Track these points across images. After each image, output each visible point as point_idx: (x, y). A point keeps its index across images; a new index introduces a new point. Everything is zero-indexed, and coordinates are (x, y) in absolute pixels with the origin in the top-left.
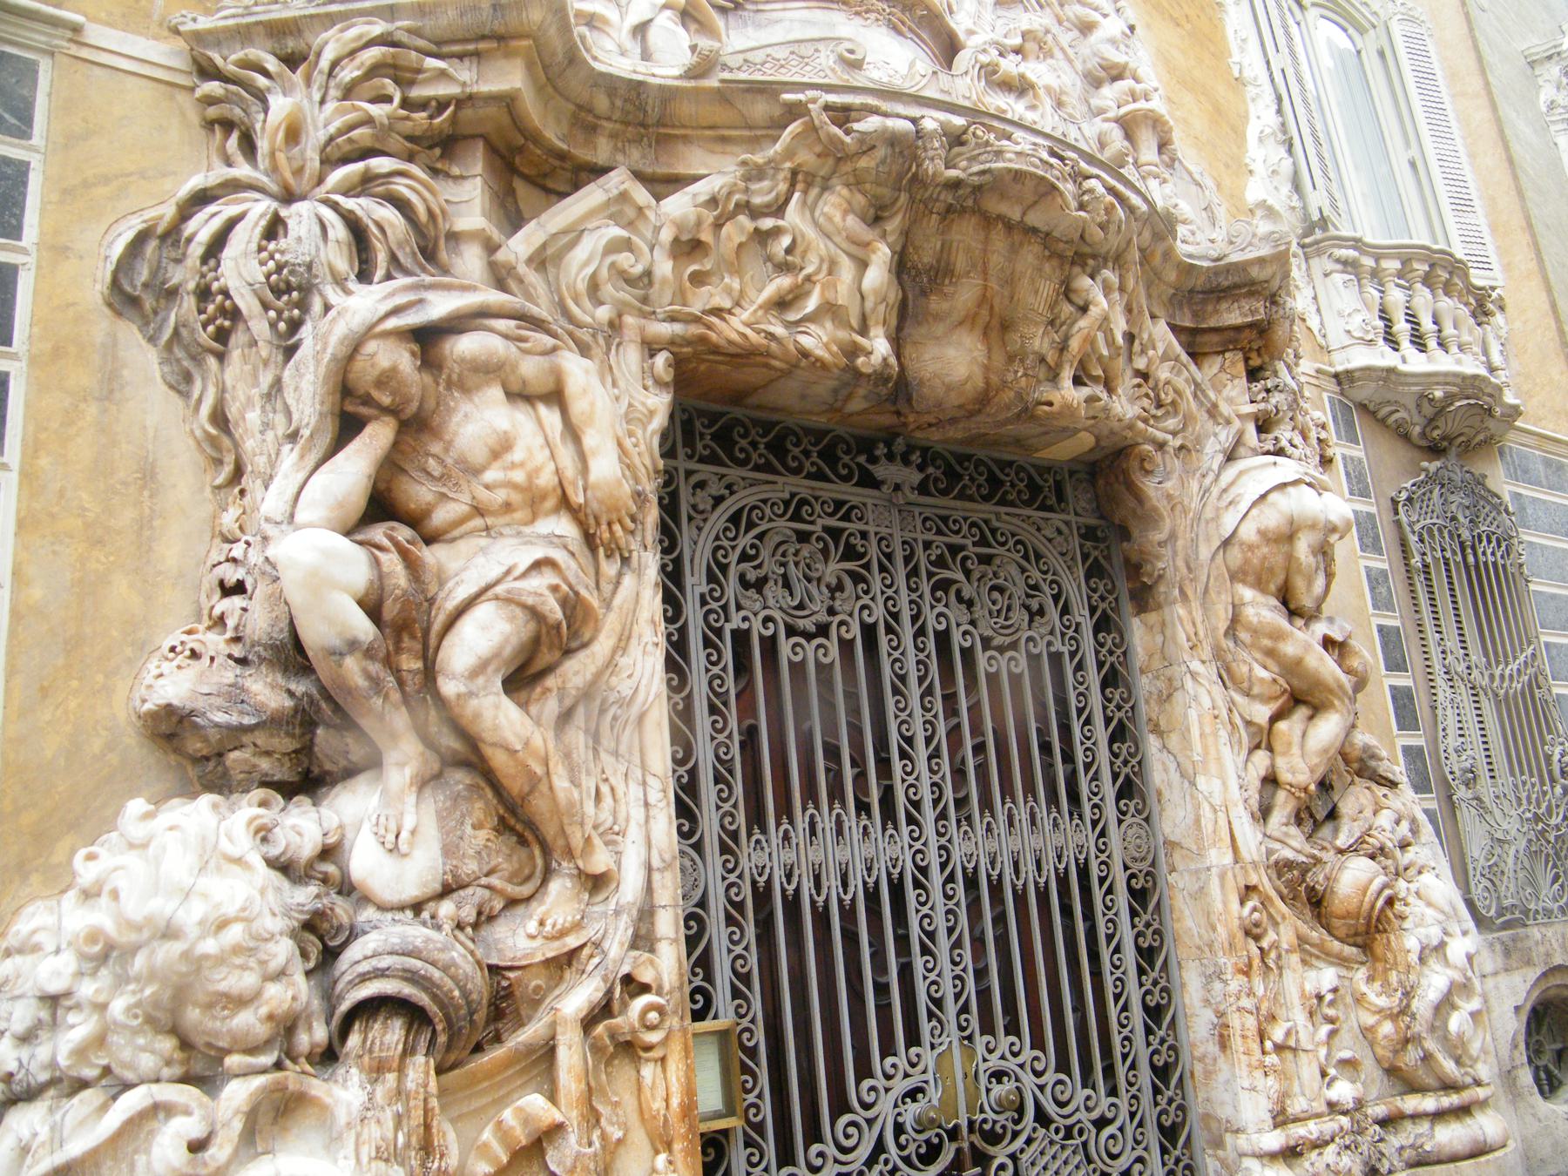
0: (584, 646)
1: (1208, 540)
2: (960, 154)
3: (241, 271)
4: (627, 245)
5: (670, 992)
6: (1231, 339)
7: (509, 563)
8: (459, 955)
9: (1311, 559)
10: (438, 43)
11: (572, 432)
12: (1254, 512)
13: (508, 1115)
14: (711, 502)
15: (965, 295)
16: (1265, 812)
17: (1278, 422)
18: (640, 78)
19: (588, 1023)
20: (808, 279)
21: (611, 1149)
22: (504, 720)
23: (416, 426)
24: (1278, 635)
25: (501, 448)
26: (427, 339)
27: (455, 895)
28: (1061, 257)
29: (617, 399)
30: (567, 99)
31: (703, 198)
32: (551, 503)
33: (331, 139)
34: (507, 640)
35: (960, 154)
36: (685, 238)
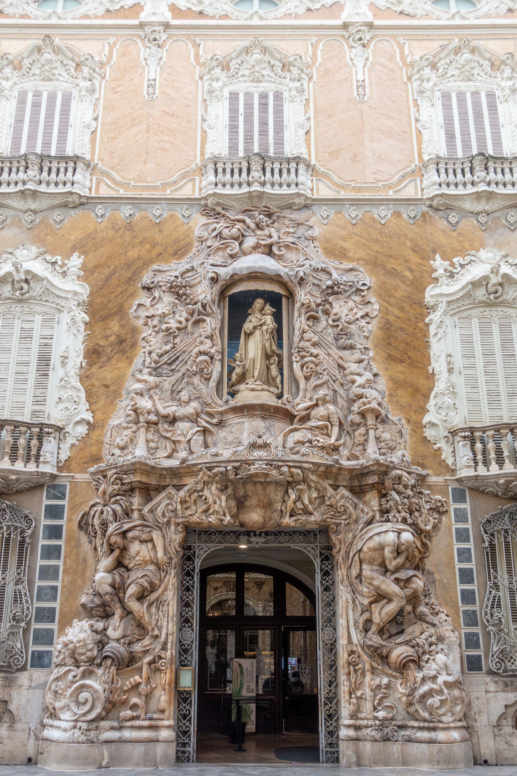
3: (96, 522)
4: (171, 504)
6: (373, 486)
8: (122, 649)
11: (154, 547)
13: (132, 679)
16: (366, 630)
19: (150, 663)
21: (153, 689)
22: (134, 605)
23: (124, 549)
25: (138, 553)
26: (124, 534)
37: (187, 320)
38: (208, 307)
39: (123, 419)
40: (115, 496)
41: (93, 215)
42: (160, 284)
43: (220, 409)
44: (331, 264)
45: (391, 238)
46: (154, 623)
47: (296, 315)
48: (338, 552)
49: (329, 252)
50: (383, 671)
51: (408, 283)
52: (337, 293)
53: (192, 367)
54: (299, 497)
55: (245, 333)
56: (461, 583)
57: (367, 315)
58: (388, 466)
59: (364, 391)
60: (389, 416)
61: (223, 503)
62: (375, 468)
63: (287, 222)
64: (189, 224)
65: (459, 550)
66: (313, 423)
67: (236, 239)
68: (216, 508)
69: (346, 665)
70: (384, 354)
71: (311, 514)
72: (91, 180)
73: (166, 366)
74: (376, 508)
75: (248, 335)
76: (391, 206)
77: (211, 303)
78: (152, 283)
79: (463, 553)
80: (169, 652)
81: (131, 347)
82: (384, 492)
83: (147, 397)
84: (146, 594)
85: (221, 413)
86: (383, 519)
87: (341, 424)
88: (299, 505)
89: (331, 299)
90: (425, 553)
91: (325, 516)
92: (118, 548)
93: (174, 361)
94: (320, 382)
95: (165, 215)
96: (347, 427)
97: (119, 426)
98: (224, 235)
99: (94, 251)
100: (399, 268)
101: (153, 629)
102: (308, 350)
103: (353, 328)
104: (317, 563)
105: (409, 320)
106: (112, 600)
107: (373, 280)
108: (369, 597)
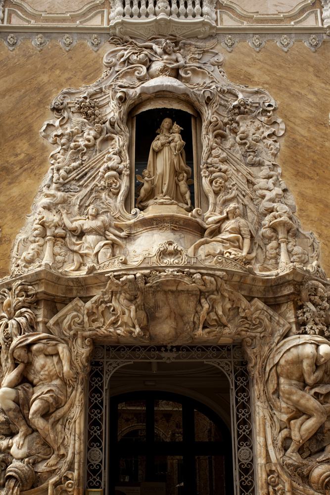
0: (62, 407)
1: (269, 365)
2: (150, 279)
4: (77, 316)
5: (75, 480)
7: (43, 391)
10: (31, 283)
11: (60, 361)
12: (285, 355)
14: (113, 368)
15: (165, 311)
17: (309, 322)
18: (77, 277)
19: (56, 484)
20: (118, 316)
22: (39, 423)
23: (29, 365)
24: (291, 393)
25: (43, 367)
26: (29, 347)
27: (29, 458)
28: (196, 295)
29: (74, 352)
30: (63, 285)
31: (93, 302)
32: (54, 378)
33: (15, 306)
34: (40, 407)
35: (150, 279)
36: (90, 311)
37: (95, 138)
38: (116, 125)
39: (30, 233)
40: (20, 309)
41: (5, 44)
42: (69, 105)
43: (128, 222)
44: (237, 88)
45: (294, 64)
46: (61, 441)
47: (204, 132)
49: (234, 77)
51: (313, 105)
52: (244, 113)
53: (100, 182)
54: (213, 307)
55: (154, 150)
57: (274, 134)
58: (303, 276)
59: (275, 205)
60: (300, 230)
61: (132, 314)
62: (291, 278)
63: (193, 49)
64: (98, 52)
66: (225, 236)
67: (144, 64)
68: (124, 320)
69: (265, 486)
70: (292, 171)
71: (225, 326)
72: (4, 12)
73: (74, 182)
74: (293, 320)
75: (156, 153)
76: (293, 35)
77: (119, 121)
78: (62, 104)
80: (76, 471)
81: (40, 165)
82: (300, 303)
83: (54, 212)
84: (51, 410)
85: (130, 227)
86: (301, 332)
87: (252, 237)
88: (213, 316)
89: (237, 118)
91: (240, 329)
92: (23, 362)
93: (82, 177)
94: (229, 196)
95: (75, 43)
96: (258, 240)
97: (25, 241)
98: (132, 61)
99: (4, 77)
100: (303, 92)
101: (59, 449)
102: (217, 165)
103: (261, 146)
104: (231, 379)
105: (315, 140)
106: (16, 417)
107: (279, 102)
108: (287, 413)
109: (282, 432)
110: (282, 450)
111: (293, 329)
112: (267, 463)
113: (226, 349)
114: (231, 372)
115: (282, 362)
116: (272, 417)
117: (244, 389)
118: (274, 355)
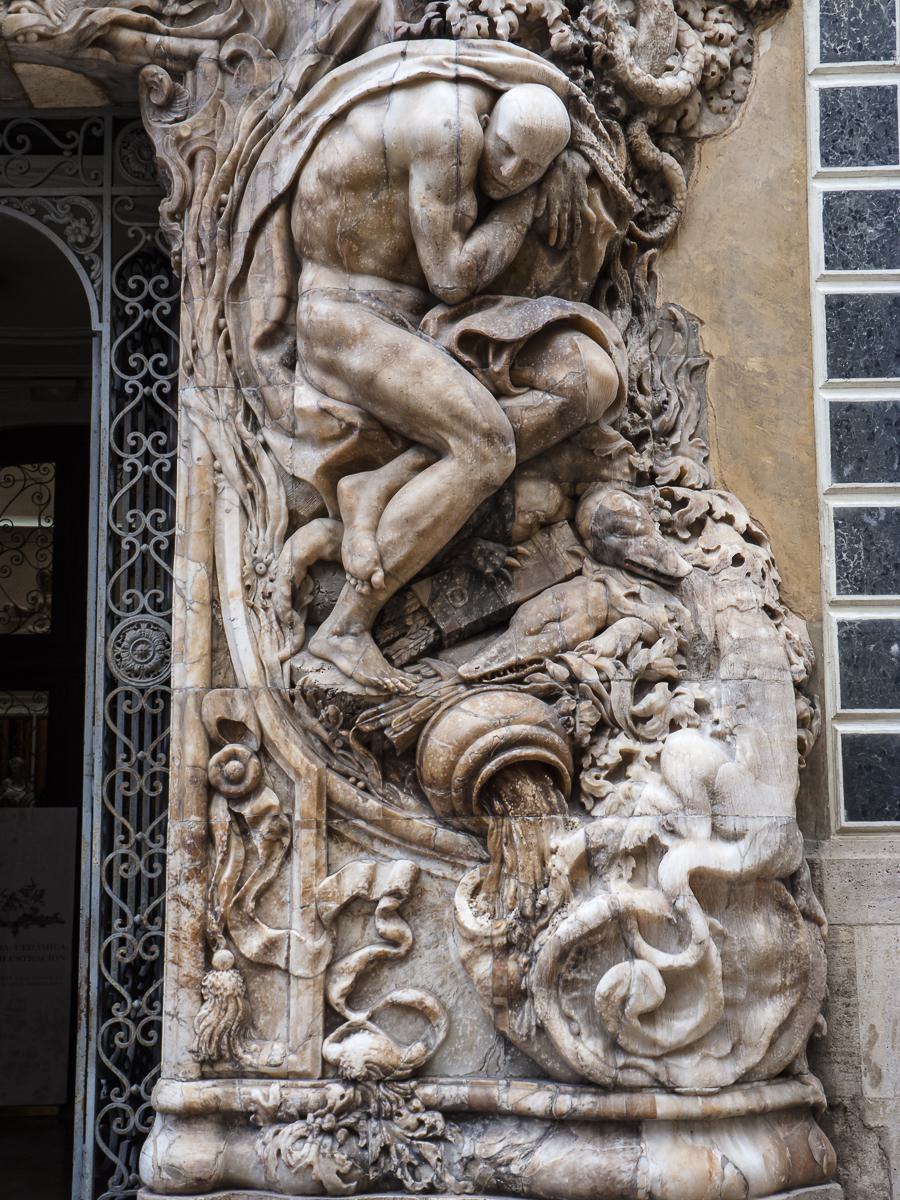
1: (254, 201)
9: (436, 208)
12: (321, 146)
48: (178, 215)
50: (385, 823)
56: (835, 370)
65: (832, 202)
69: (192, 798)
79: (858, 216)
90: (647, 221)
109: (302, 532)
110: (292, 626)
111: (383, 13)
112: (212, 687)
113: (80, 140)
114: (99, 251)
115: (309, 184)
116: (253, 463)
117: (154, 339)
118: (278, 150)
